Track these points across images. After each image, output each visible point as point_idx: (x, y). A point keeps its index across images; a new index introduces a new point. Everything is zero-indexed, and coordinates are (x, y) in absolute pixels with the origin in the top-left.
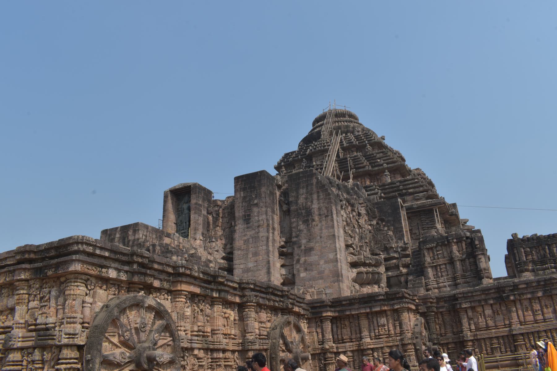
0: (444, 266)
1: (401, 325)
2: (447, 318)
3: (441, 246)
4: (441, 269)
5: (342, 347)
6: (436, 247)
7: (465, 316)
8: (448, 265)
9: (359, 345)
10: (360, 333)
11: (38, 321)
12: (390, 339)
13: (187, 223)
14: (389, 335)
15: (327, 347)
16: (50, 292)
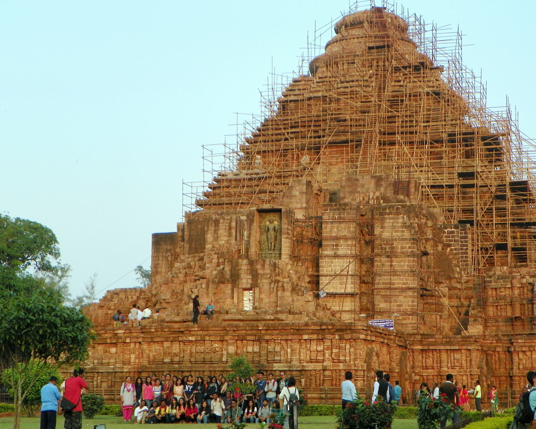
0: (505, 307)
1: (471, 361)
2: (503, 356)
3: (505, 288)
4: (501, 309)
5: (425, 373)
6: (500, 288)
7: (517, 357)
8: (508, 306)
9: (440, 372)
10: (440, 364)
11: (341, 359)
12: (462, 370)
13: (273, 244)
14: (461, 367)
15: (417, 371)
16: (345, 346)
